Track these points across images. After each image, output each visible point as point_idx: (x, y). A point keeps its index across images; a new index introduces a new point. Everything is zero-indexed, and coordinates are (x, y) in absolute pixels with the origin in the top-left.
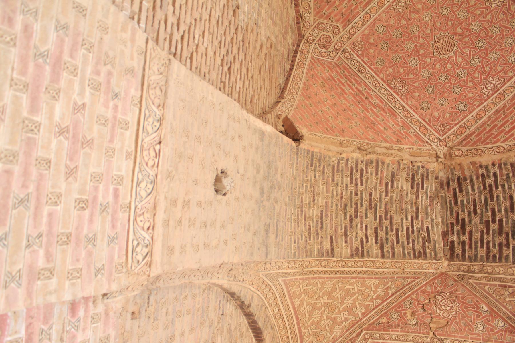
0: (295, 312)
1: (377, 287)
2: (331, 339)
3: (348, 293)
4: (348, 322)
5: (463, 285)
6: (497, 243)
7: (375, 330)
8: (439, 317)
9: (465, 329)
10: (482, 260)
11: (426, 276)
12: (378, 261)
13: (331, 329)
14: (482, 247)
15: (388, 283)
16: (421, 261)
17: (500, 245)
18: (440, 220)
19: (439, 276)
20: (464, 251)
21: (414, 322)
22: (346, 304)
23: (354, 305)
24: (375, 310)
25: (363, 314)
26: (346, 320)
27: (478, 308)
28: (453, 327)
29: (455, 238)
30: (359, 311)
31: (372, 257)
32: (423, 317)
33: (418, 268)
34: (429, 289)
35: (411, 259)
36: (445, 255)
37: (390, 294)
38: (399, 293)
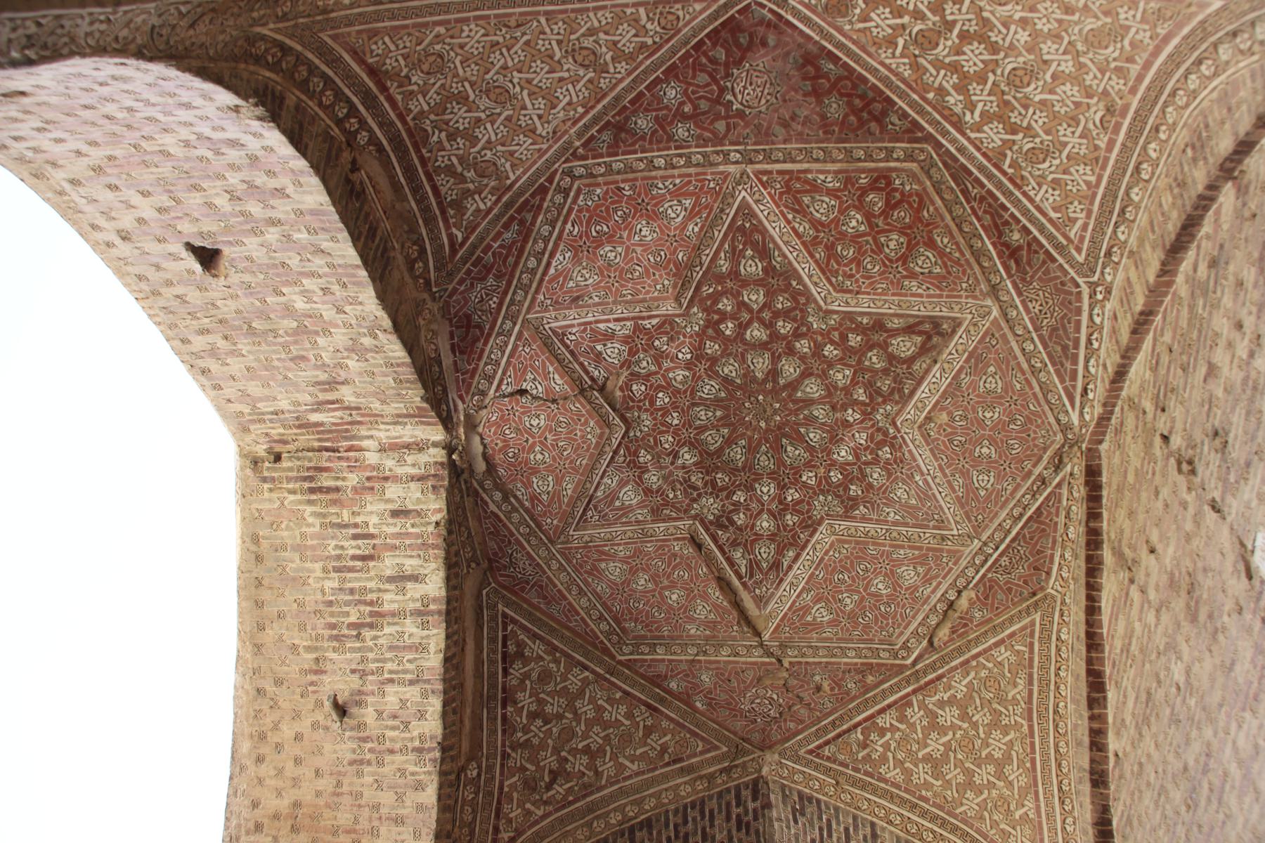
0: (1036, 785)
1: (884, 759)
2: (972, 674)
3: (936, 764)
4: (937, 697)
5: (735, 733)
6: (690, 824)
7: (886, 665)
8: (773, 688)
9: (730, 674)
10: (710, 798)
11: (796, 751)
12: (881, 819)
13: (971, 697)
14: (711, 812)
15: (863, 758)
16: (807, 791)
17: (686, 822)
18: (776, 824)
19: (775, 744)
20: (738, 796)
21: (817, 678)
22: (941, 741)
23: (927, 731)
24: (886, 702)
25: (910, 704)
26: (941, 704)
27: (709, 704)
28: (750, 675)
29: (751, 805)
30: (915, 714)
31: (891, 832)
32: (802, 686)
33: (811, 778)
34: (792, 725)
35: (825, 802)
36: (767, 783)
37: (859, 730)
38: (845, 727)
